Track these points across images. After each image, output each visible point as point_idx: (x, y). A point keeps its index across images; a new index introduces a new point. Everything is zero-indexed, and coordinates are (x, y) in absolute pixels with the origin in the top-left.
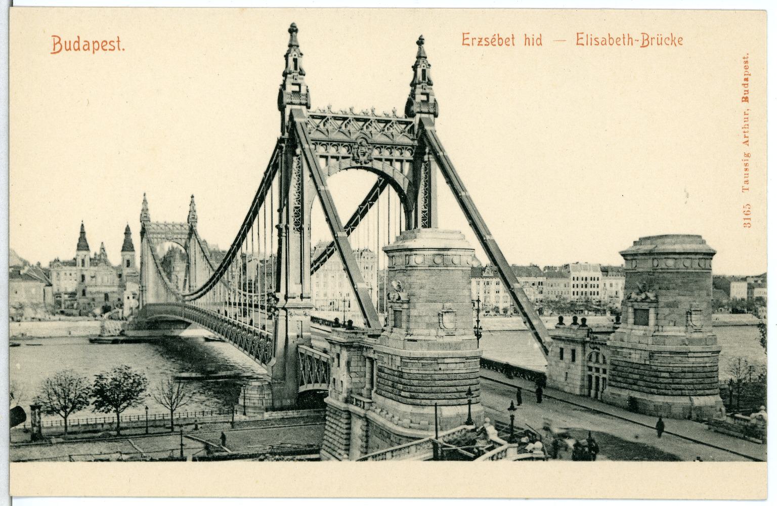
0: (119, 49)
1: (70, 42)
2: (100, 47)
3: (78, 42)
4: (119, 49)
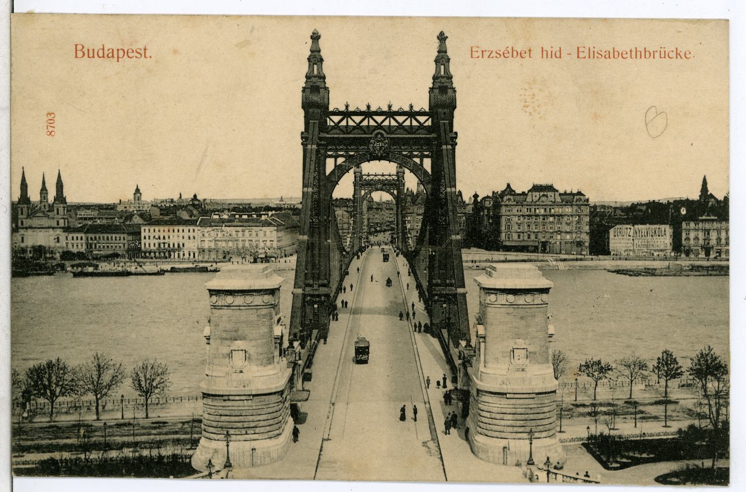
0: (145, 57)
1: (93, 50)
2: (126, 54)
3: (103, 49)
4: (145, 57)
